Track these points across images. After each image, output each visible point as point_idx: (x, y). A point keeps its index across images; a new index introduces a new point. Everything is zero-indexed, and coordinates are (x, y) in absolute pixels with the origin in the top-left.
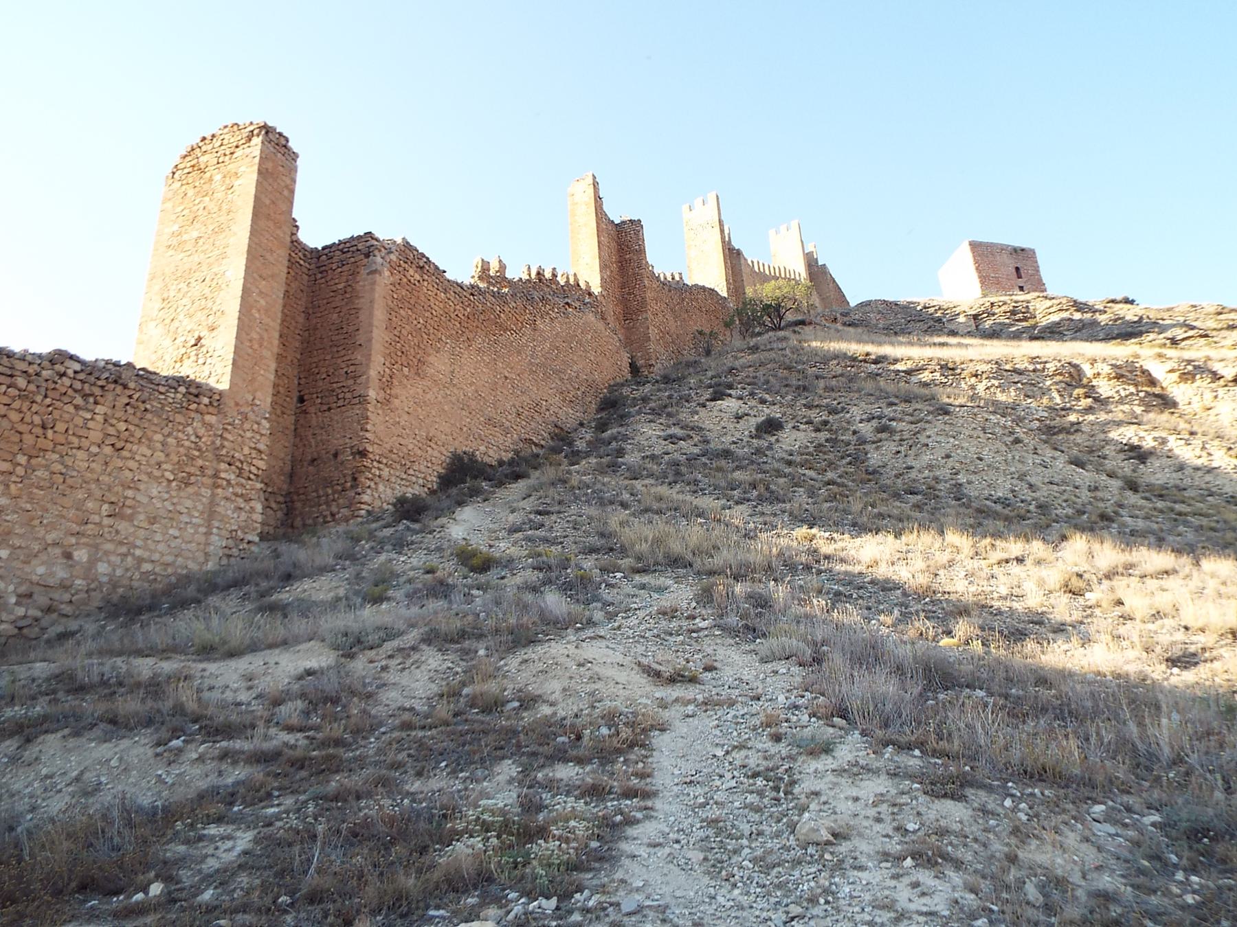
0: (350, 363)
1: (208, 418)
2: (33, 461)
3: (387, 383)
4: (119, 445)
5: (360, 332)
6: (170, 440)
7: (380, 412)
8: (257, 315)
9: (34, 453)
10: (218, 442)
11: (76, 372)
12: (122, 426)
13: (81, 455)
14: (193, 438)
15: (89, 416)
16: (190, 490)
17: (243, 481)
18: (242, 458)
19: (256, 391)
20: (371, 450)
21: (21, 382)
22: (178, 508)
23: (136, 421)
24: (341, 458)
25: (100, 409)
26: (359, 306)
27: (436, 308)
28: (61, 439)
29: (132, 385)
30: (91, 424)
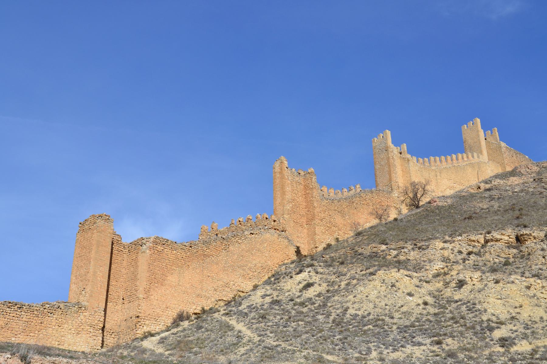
0: (135, 286)
1: (84, 314)
2: (39, 332)
3: (147, 291)
4: (60, 326)
5: (139, 274)
6: (73, 322)
7: (145, 302)
8: (99, 279)
9: (40, 330)
10: (87, 321)
11: (48, 307)
12: (60, 320)
13: (50, 329)
14: (80, 320)
15: (52, 318)
16: (79, 335)
17: (95, 331)
18: (95, 324)
19: (99, 303)
20: (141, 315)
21: (35, 312)
22: (76, 341)
23: (64, 318)
24: (132, 319)
25: (55, 316)
26: (138, 265)
27: (171, 258)
28: (45, 326)
29: (63, 308)
30: (52, 321)
